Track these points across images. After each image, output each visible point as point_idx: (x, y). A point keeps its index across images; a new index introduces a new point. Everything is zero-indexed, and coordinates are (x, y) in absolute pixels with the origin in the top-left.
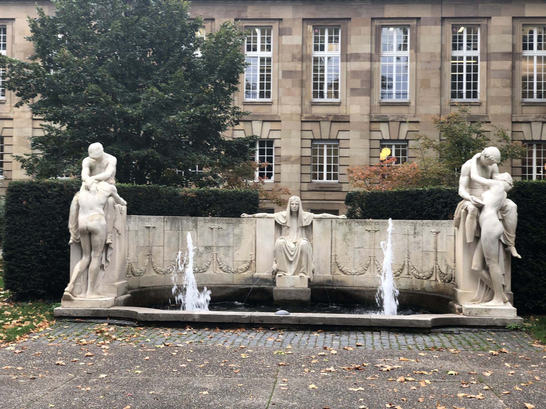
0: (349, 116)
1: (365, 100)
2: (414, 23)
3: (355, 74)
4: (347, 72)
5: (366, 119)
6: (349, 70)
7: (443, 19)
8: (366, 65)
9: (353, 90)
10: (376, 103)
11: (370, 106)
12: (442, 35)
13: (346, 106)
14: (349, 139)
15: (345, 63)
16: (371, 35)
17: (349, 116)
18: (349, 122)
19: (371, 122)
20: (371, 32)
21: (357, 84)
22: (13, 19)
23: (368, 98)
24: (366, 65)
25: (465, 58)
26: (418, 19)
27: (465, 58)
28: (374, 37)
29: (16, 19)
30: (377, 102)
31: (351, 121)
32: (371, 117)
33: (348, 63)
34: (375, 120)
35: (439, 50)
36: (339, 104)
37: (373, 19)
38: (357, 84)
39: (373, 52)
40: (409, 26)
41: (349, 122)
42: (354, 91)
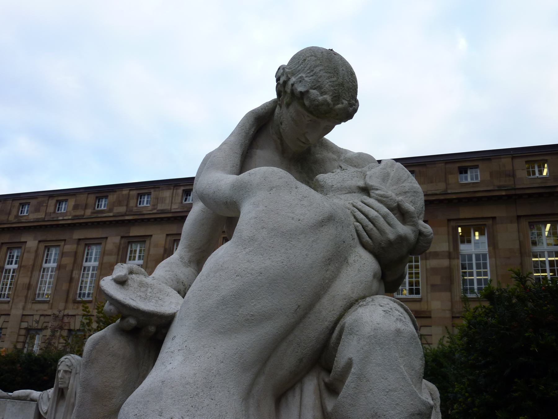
0: (430, 312)
1: (446, 295)
2: (490, 222)
3: (434, 271)
4: (426, 269)
5: (448, 315)
6: (428, 267)
7: (519, 217)
8: (445, 263)
9: (433, 286)
10: (457, 299)
11: (452, 302)
12: (519, 232)
13: (427, 301)
14: (431, 335)
15: (424, 261)
16: (448, 234)
17: (430, 312)
18: (430, 317)
19: (453, 317)
20: (448, 232)
21: (437, 280)
22: (151, 236)
23: (448, 294)
24: (445, 263)
25: (546, 254)
26: (494, 218)
27: (546, 254)
28: (451, 237)
29: (153, 236)
30: (458, 297)
31: (432, 316)
32: (452, 311)
33: (428, 261)
34: (457, 315)
35: (517, 246)
36: (420, 300)
37: (449, 220)
38: (437, 280)
39: (452, 250)
40: (485, 225)
41: (430, 317)
42: (434, 288)
